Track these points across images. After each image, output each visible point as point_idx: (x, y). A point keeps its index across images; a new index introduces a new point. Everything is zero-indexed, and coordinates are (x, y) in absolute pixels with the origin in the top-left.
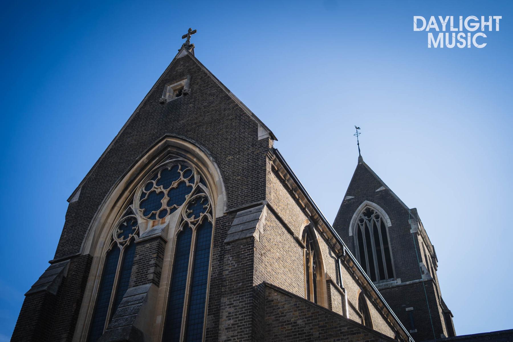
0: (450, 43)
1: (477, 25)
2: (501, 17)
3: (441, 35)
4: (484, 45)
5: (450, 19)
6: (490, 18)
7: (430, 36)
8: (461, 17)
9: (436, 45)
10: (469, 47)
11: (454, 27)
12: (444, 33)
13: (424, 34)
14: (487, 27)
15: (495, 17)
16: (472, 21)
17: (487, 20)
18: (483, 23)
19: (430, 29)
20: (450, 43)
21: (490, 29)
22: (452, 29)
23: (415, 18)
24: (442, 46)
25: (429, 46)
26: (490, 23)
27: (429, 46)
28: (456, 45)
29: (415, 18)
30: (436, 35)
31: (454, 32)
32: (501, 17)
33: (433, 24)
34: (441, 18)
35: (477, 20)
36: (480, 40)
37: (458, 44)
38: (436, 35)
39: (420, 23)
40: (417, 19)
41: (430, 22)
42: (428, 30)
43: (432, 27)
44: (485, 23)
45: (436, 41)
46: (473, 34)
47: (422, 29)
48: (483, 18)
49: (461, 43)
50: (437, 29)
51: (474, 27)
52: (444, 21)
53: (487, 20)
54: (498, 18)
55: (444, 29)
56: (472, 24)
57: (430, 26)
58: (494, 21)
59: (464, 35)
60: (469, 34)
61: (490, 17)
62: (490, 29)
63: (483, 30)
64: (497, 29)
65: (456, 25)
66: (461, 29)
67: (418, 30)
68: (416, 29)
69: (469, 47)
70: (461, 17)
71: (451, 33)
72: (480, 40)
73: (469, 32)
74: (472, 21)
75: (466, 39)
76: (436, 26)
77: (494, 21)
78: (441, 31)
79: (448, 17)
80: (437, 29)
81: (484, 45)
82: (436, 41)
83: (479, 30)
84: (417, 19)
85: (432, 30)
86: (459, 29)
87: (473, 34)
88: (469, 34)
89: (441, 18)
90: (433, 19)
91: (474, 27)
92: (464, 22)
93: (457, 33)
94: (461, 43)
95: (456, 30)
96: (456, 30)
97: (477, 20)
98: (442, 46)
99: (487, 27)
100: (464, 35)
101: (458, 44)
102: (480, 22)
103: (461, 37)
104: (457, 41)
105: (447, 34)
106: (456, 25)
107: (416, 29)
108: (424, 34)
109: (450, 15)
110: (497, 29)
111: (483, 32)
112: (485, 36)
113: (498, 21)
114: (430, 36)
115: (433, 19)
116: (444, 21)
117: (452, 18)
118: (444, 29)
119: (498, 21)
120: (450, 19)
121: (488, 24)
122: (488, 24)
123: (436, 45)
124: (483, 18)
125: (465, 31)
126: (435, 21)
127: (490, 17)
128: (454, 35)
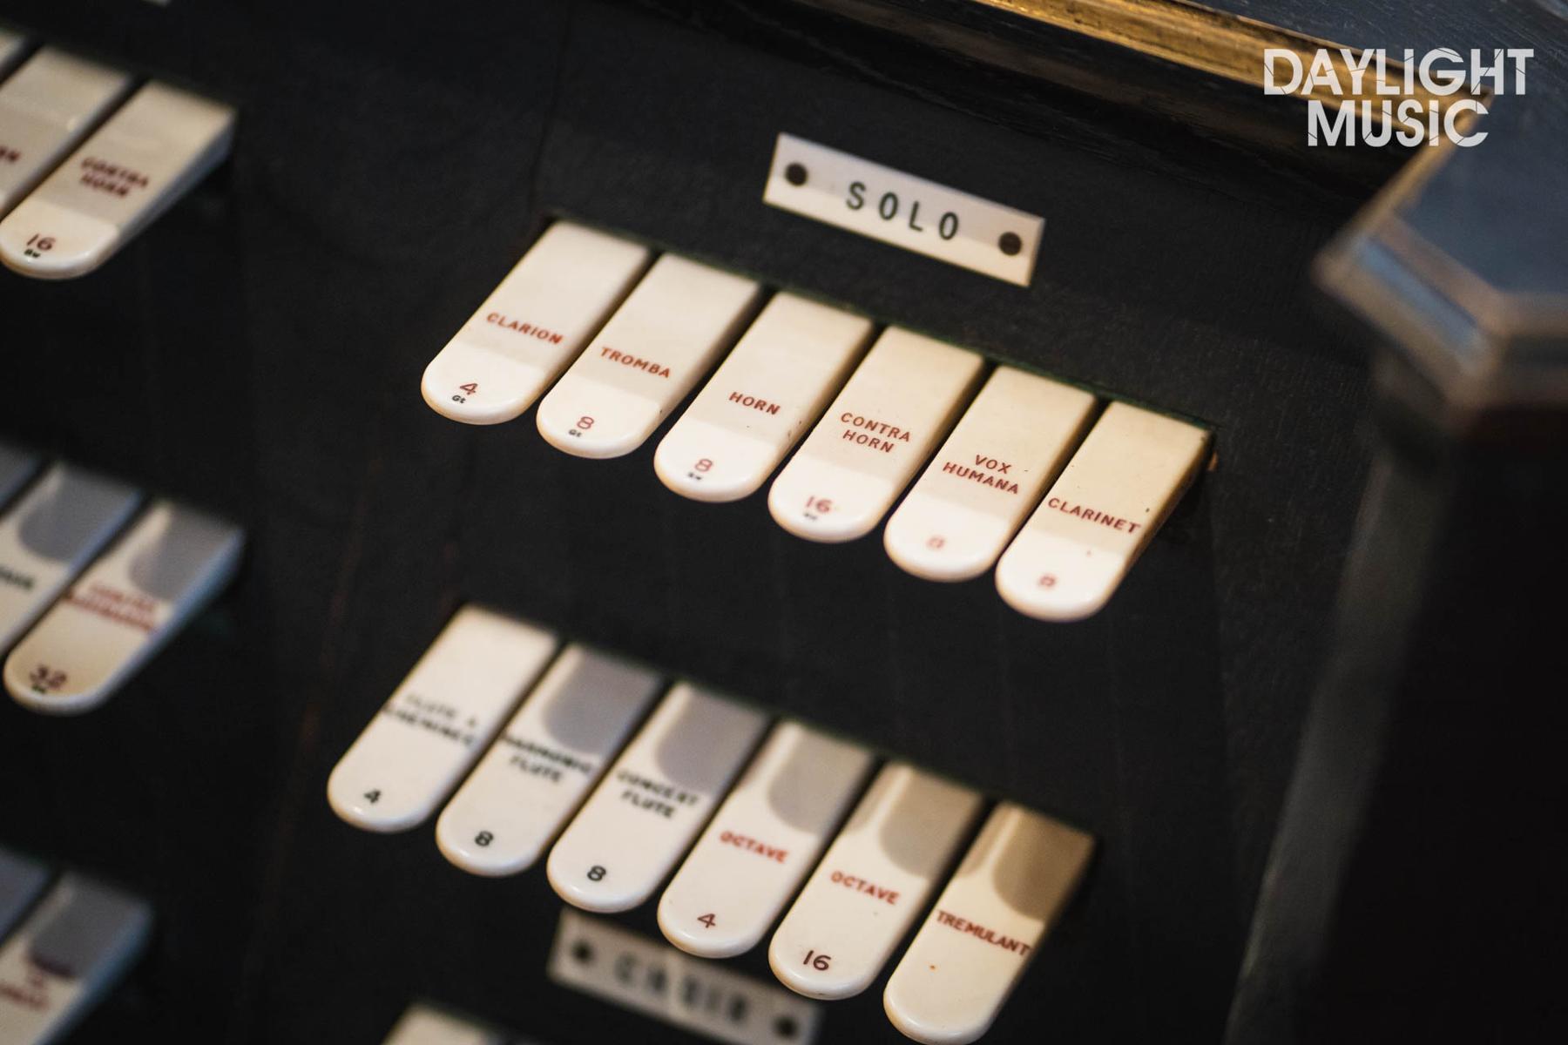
1: (1458, 78)
2: (1530, 53)
4: (1480, 137)
6: (1499, 55)
7: (1315, 110)
8: (1409, 53)
9: (1332, 139)
14: (1488, 82)
15: (1512, 53)
17: (1487, 61)
18: (1478, 71)
21: (1499, 89)
24: (1350, 141)
25: (1313, 141)
26: (1497, 72)
27: (1313, 141)
32: (1530, 53)
33: (1322, 73)
35: (1460, 60)
37: (1401, 137)
39: (1283, 73)
41: (1315, 69)
45: (1332, 126)
47: (1289, 89)
48: (1476, 54)
50: (1337, 91)
53: (1487, 61)
54: (1521, 55)
55: (1357, 89)
56: (1441, 74)
57: (1314, 80)
58: (1510, 64)
61: (1497, 51)
62: (1499, 89)
63: (1476, 89)
64: (1521, 89)
70: (1409, 53)
73: (1435, 97)
75: (1424, 119)
77: (1510, 64)
79: (1367, 54)
80: (1337, 91)
81: (1480, 137)
82: (1332, 126)
83: (1465, 91)
86: (1402, 90)
89: (1346, 53)
90: (1322, 57)
91: (1445, 82)
94: (1410, 135)
95: (1395, 91)
97: (1460, 60)
98: (1350, 141)
99: (1488, 82)
100: (1419, 109)
102: (1466, 66)
103: (1410, 113)
105: (1367, 104)
109: (1375, 47)
110: (1521, 89)
111: (1476, 98)
112: (1481, 110)
113: (1521, 65)
118: (1357, 89)
119: (1521, 65)
121: (1491, 72)
122: (1491, 72)
123: (1332, 139)
124: (1476, 54)
125: (1423, 96)
127: (1497, 51)
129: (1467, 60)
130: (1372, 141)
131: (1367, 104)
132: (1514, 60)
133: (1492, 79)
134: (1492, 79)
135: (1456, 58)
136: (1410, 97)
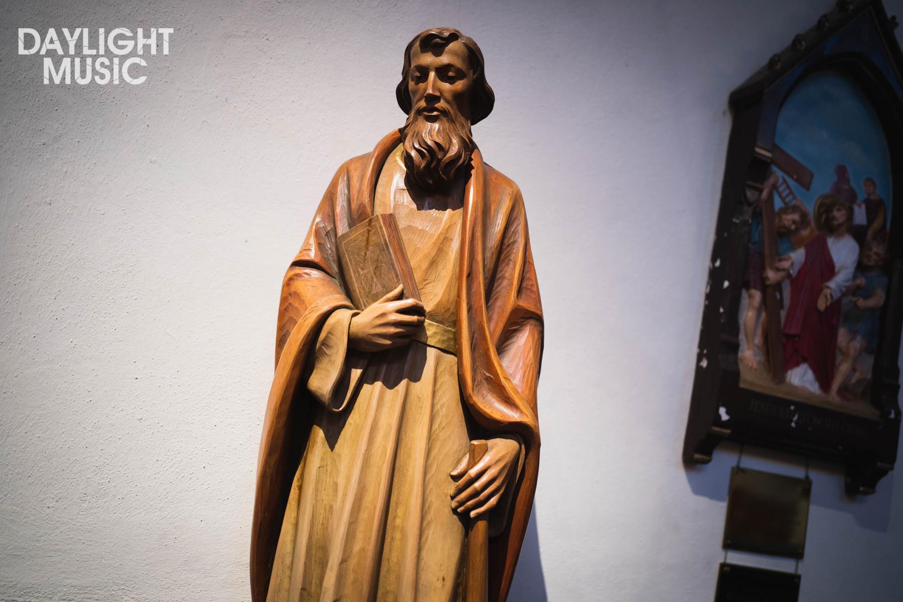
0: (83, 76)
1: (130, 44)
2: (171, 30)
3: (66, 62)
5: (82, 33)
6: (153, 32)
7: (48, 63)
8: (102, 31)
9: (57, 80)
10: (116, 82)
11: (90, 47)
12: (73, 58)
13: (37, 59)
14: (147, 47)
15: (161, 30)
16: (121, 37)
17: (147, 36)
18: (141, 41)
19: (48, 50)
20: (83, 76)
21: (154, 51)
22: (86, 51)
23: (22, 32)
24: (68, 81)
25: (46, 82)
26: (153, 41)
27: (46, 82)
28: (93, 79)
29: (22, 32)
30: (57, 63)
31: (90, 56)
33: (52, 42)
34: (66, 31)
35: (128, 33)
36: (135, 71)
37: (97, 78)
38: (57, 63)
39: (29, 42)
40: (26, 35)
41: (47, 40)
42: (43, 52)
43: (51, 47)
44: (145, 41)
45: (57, 73)
46: (123, 59)
47: (33, 51)
48: (140, 31)
49: (102, 76)
50: (60, 52)
51: (123, 47)
52: (72, 37)
53: (147, 36)
54: (166, 32)
55: (72, 51)
56: (120, 43)
57: (47, 46)
58: (160, 37)
59: (107, 62)
60: (116, 60)
61: (152, 29)
62: (154, 51)
63: (141, 53)
64: (166, 51)
65: (94, 44)
66: (102, 52)
67: (26, 52)
68: (22, 51)
69: (116, 82)
70: (102, 31)
71: (83, 59)
72: (135, 71)
73: (116, 56)
74: (121, 37)
76: (57, 46)
77: (160, 37)
78: (66, 54)
79: (78, 31)
80: (60, 52)
81: (142, 79)
82: (57, 73)
83: (133, 53)
84: (26, 35)
85: (51, 53)
86: (98, 52)
87: (123, 59)
88: (116, 60)
89: (66, 31)
90: (52, 33)
91: (123, 47)
92: (107, 39)
93: (95, 58)
94: (102, 76)
95: (94, 52)
96: (94, 52)
97: (131, 35)
98: (68, 81)
99: (147, 47)
100: (107, 62)
101: (97, 78)
102: (134, 38)
103: (102, 64)
104: (95, 72)
105: (77, 61)
106: (94, 44)
107: (22, 51)
108: (37, 59)
110: (166, 51)
113: (166, 38)
114: (48, 63)
115: (52, 33)
116: (72, 37)
117: (86, 31)
118: (72, 51)
119: (166, 38)
120: (82, 33)
121: (149, 42)
122: (149, 42)
123: (57, 80)
124: (140, 31)
125: (108, 54)
126: (55, 38)
127: (152, 29)
128: (89, 61)
129: (135, 33)
130: (81, 82)
131: (77, 61)
132: (162, 34)
133: (150, 45)
134: (150, 45)
135: (128, 33)
136: (102, 56)
